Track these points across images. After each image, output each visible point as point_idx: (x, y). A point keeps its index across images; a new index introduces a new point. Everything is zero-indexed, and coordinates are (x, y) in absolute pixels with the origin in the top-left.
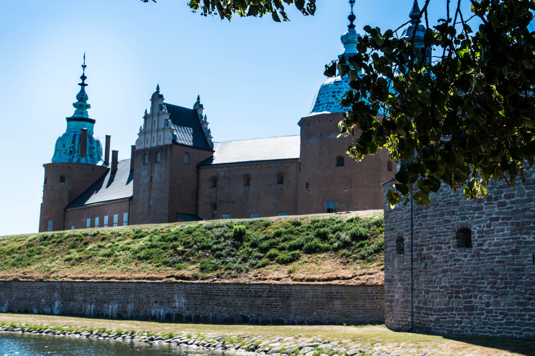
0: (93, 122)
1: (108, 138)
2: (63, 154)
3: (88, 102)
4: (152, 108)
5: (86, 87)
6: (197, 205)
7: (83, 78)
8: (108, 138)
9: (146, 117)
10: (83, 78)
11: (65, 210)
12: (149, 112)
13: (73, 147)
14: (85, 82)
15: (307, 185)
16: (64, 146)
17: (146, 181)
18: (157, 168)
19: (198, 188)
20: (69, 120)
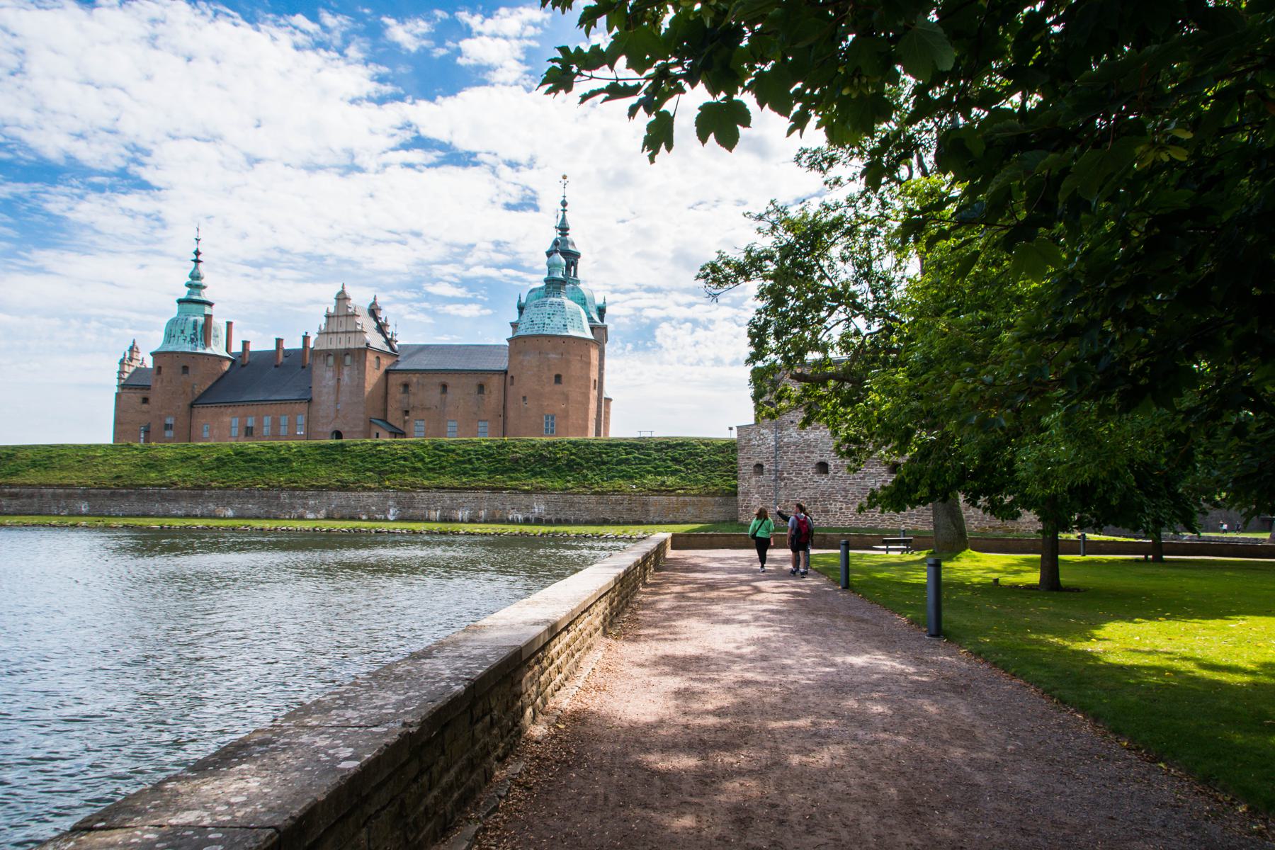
0: (210, 304)
1: (229, 324)
2: (181, 341)
3: (203, 282)
4: (337, 307)
5: (201, 265)
6: (385, 410)
7: (197, 253)
8: (229, 324)
9: (328, 316)
10: (197, 253)
11: (192, 406)
12: (332, 310)
13: (195, 334)
14: (200, 258)
15: (524, 398)
16: (182, 332)
17: (332, 383)
18: (346, 371)
19: (386, 393)
20: (180, 302)
